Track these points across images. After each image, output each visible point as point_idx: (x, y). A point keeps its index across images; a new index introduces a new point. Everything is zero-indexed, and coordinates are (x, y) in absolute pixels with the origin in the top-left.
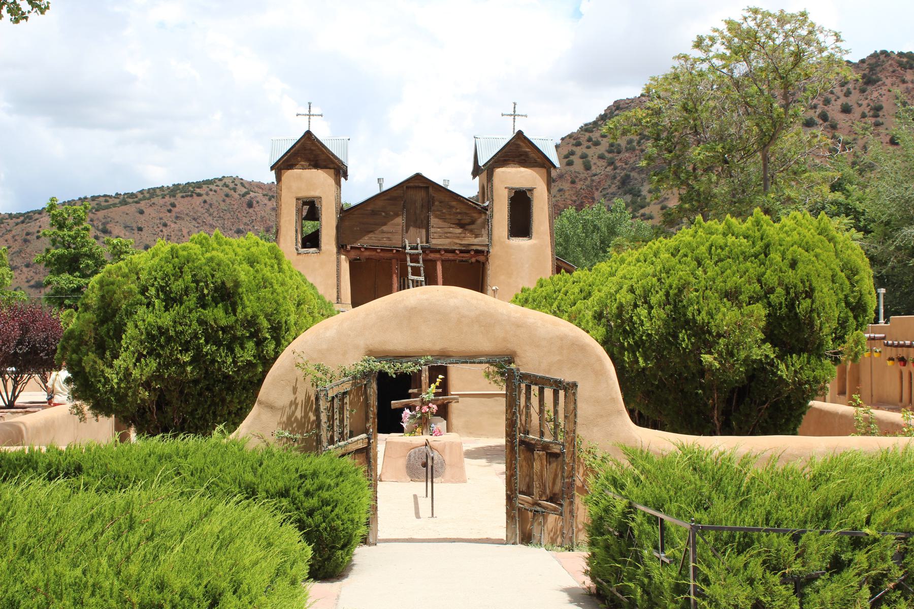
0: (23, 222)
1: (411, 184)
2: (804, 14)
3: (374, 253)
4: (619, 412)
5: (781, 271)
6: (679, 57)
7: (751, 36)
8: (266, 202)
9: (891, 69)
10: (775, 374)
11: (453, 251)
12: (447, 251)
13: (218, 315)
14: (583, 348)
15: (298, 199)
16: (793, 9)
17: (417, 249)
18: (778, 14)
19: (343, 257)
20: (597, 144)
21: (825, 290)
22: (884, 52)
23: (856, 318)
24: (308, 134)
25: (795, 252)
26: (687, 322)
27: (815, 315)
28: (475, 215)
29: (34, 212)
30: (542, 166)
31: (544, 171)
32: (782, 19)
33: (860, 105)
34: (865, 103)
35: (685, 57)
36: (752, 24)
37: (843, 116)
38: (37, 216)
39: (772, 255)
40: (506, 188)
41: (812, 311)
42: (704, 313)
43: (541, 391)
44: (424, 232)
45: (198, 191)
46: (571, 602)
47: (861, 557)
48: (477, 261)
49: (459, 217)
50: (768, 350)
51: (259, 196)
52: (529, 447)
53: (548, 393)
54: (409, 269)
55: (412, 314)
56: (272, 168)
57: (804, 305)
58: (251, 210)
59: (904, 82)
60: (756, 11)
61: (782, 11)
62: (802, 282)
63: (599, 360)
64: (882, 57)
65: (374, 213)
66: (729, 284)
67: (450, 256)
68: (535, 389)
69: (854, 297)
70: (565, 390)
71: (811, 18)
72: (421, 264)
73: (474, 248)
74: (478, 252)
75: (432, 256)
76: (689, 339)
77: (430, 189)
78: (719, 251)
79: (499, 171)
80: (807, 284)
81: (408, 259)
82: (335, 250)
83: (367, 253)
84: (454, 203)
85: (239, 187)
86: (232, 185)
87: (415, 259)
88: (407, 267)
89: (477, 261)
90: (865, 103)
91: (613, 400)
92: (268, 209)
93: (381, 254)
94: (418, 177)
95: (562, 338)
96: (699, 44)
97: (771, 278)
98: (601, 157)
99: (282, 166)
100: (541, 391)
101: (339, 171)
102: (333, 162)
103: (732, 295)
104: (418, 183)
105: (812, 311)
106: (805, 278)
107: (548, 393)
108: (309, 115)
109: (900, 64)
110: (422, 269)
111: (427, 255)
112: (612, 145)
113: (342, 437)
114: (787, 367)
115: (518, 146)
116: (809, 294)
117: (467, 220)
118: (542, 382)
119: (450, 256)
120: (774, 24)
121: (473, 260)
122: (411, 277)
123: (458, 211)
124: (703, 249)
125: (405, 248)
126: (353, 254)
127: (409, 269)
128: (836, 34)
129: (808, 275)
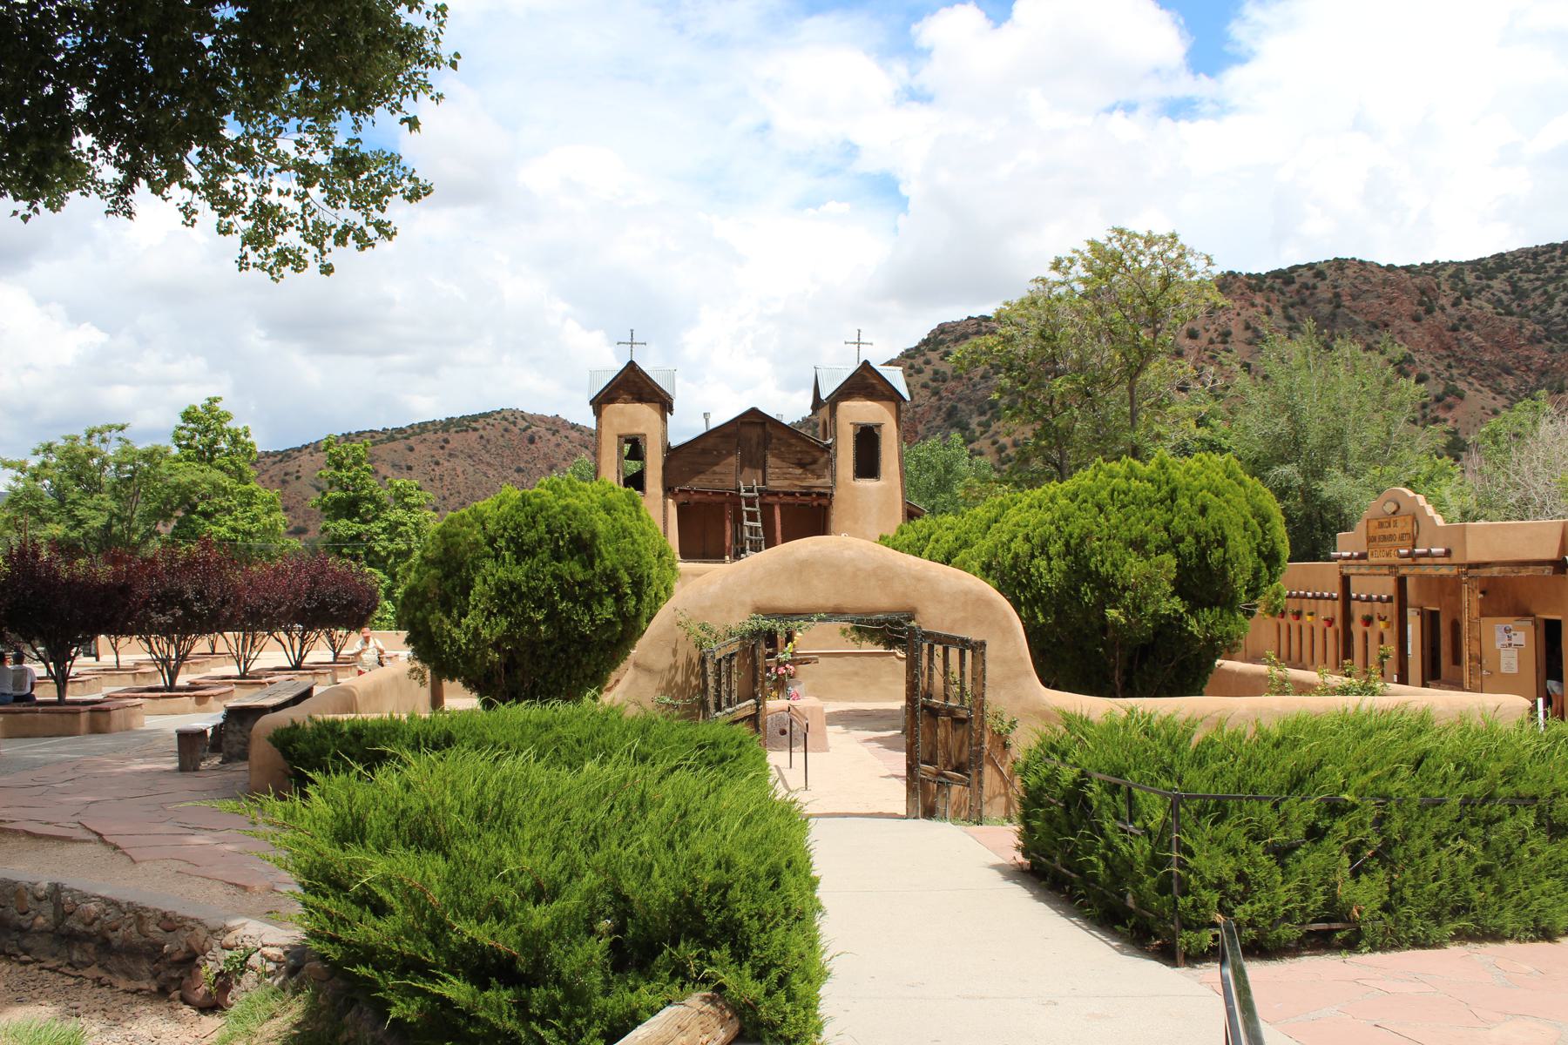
0: (281, 461)
2: (1173, 236)
3: (704, 496)
4: (1028, 674)
5: (1190, 518)
6: (1036, 281)
7: (1117, 258)
8: (550, 437)
9: (1239, 292)
10: (1185, 630)
11: (793, 494)
12: (786, 494)
13: (572, 569)
14: (989, 604)
15: (620, 436)
16: (1161, 230)
17: (752, 491)
18: (1145, 234)
19: (670, 501)
20: (920, 371)
21: (1238, 538)
22: (1231, 273)
23: (1269, 568)
24: (632, 365)
25: (1204, 497)
26: (1089, 573)
27: (1229, 566)
28: (817, 454)
29: (293, 450)
30: (890, 399)
31: (892, 405)
32: (1150, 241)
33: (1208, 331)
34: (1212, 328)
35: (1044, 281)
36: (1116, 245)
37: (1188, 342)
38: (296, 454)
39: (1179, 501)
41: (1225, 561)
42: (1108, 564)
43: (946, 651)
44: (760, 472)
45: (474, 425)
46: (1006, 880)
47: (1341, 825)
48: (819, 505)
49: (799, 456)
50: (1177, 604)
51: (542, 431)
52: (933, 712)
53: (954, 653)
54: (745, 514)
55: (803, 567)
57: (1216, 554)
58: (533, 447)
59: (1253, 305)
60: (1121, 232)
61: (1150, 232)
62: (1214, 529)
63: (1006, 616)
64: (1230, 278)
65: (704, 452)
66: (1135, 533)
67: (789, 499)
68: (939, 649)
69: (1266, 546)
70: (973, 651)
71: (1181, 240)
72: (757, 509)
73: (816, 490)
74: (820, 495)
75: (769, 499)
76: (1092, 593)
78: (1122, 496)
79: (844, 406)
80: (1219, 532)
82: (661, 493)
83: (697, 497)
84: (793, 441)
85: (520, 420)
86: (511, 419)
87: (750, 503)
88: (742, 511)
89: (819, 505)
90: (1212, 328)
91: (1021, 660)
92: (552, 445)
93: (713, 498)
94: (754, 412)
95: (966, 593)
96: (1056, 265)
97: (1179, 525)
98: (925, 386)
99: (600, 403)
100: (946, 651)
101: (665, 404)
102: (658, 395)
103: (1138, 545)
104: (754, 419)
105: (1225, 561)
106: (1217, 526)
107: (954, 653)
108: (632, 344)
109: (1249, 287)
112: (936, 372)
113: (730, 704)
114: (1198, 622)
115: (864, 378)
116: (1222, 542)
117: (808, 459)
118: (947, 641)
119: (789, 499)
120: (1141, 245)
121: (815, 504)
122: (746, 523)
124: (1105, 494)
125: (739, 490)
126: (682, 498)
127: (745, 514)
128: (1208, 258)
129: (1219, 522)
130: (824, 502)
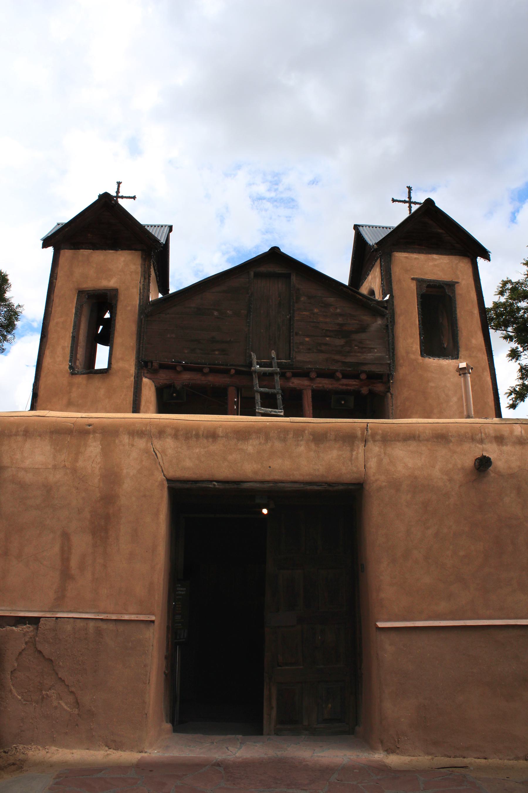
1: (263, 269)
17: (270, 365)
28: (366, 318)
40: (413, 279)
48: (371, 392)
49: (340, 320)
56: (47, 242)
67: (325, 384)
73: (366, 368)
74: (373, 377)
75: (296, 383)
77: (294, 278)
81: (256, 381)
82: (132, 370)
83: (186, 377)
89: (371, 392)
110: (279, 397)
111: (288, 379)
121: (365, 391)
123: (338, 310)
125: (251, 365)
126: (164, 377)
127: (258, 397)
130: (379, 388)
